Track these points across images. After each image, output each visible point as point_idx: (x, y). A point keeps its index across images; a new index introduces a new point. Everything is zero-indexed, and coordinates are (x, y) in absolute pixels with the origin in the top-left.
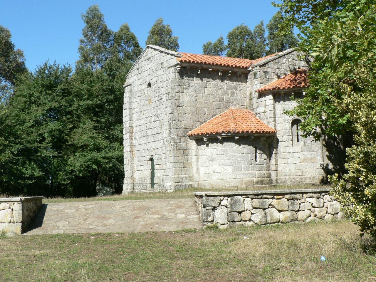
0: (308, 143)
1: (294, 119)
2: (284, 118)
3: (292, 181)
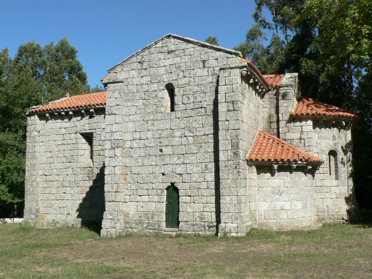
2: (321, 148)
3: (331, 218)
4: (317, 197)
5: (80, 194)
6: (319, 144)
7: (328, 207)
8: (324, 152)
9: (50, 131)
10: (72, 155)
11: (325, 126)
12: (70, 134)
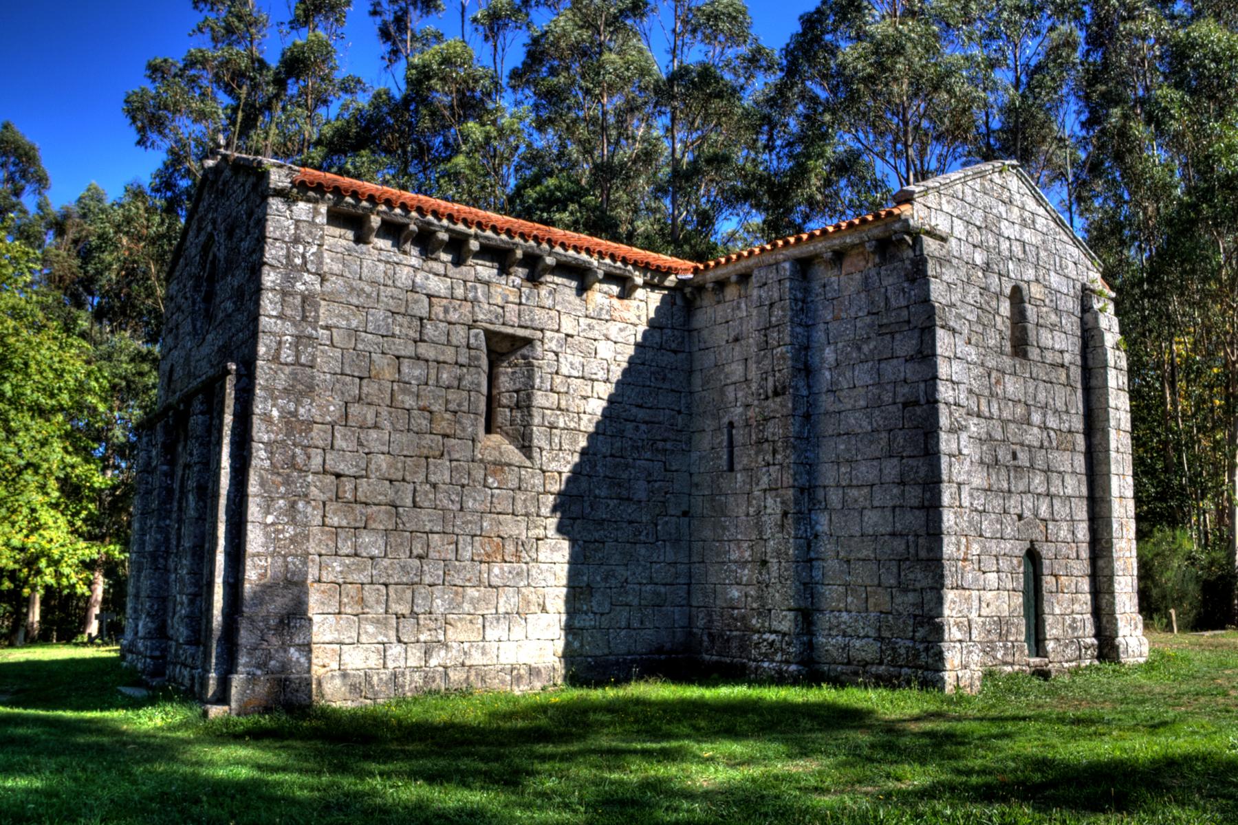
5: (481, 562)
9: (367, 289)
10: (453, 406)
12: (450, 323)
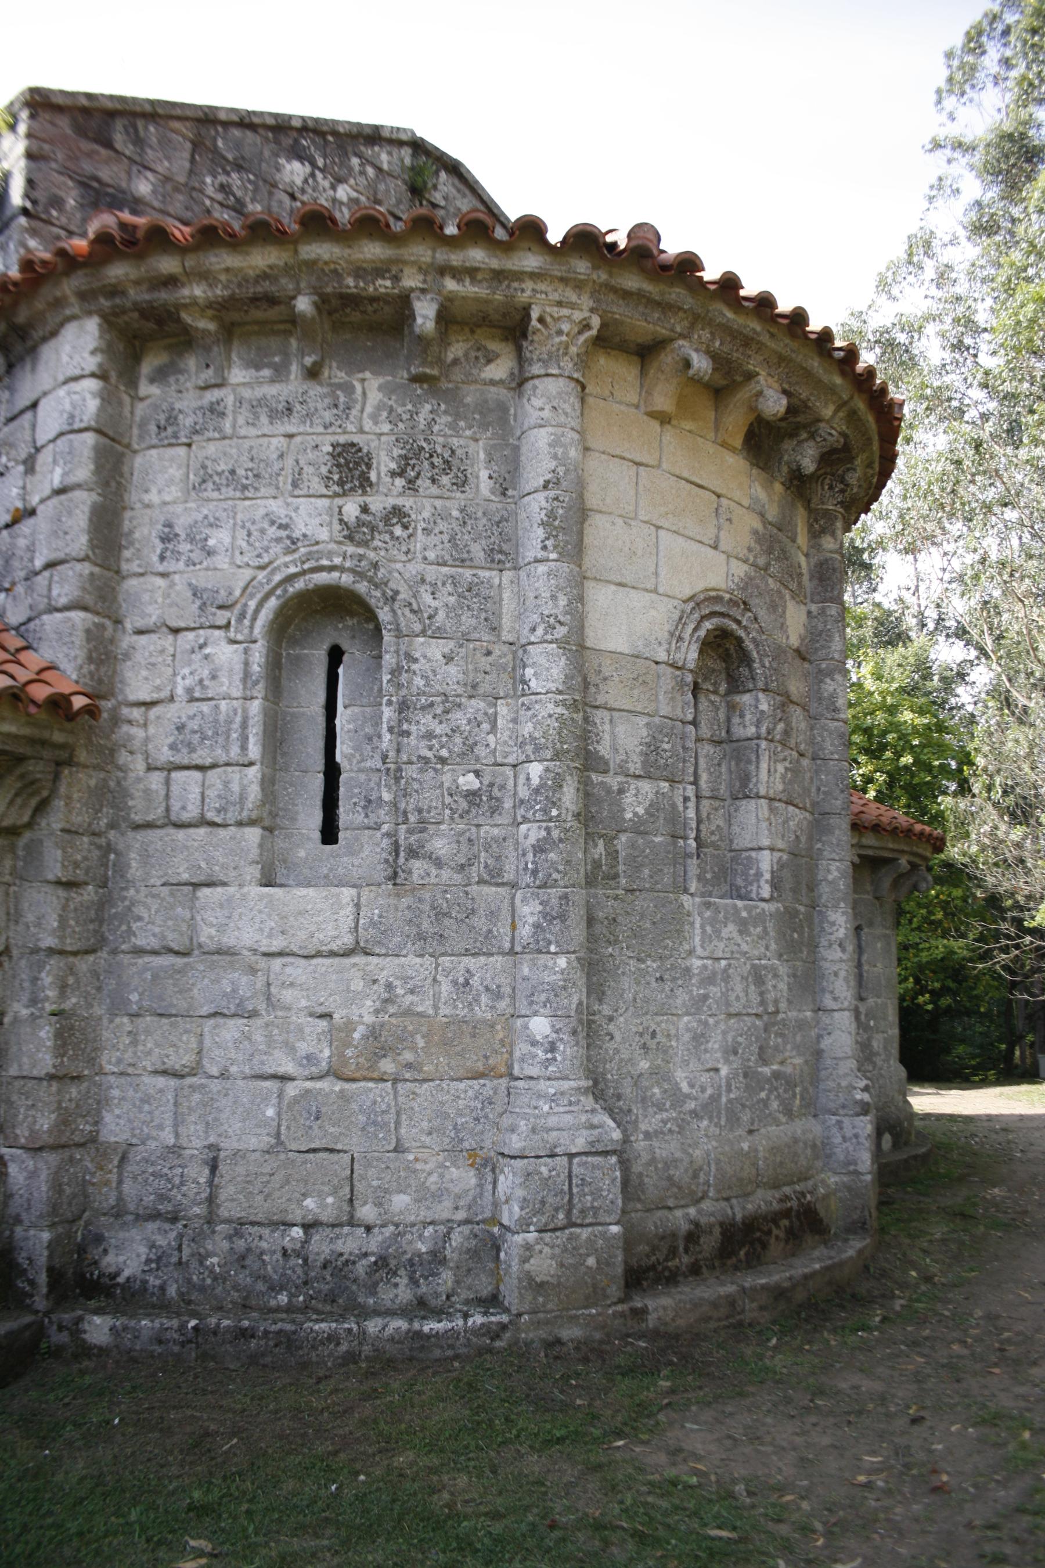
0: (438, 863)
1: (300, 585)
2: (203, 579)
4: (128, 1056)
6: (185, 547)
7: (214, 1166)
8: (221, 617)
11: (258, 367)
